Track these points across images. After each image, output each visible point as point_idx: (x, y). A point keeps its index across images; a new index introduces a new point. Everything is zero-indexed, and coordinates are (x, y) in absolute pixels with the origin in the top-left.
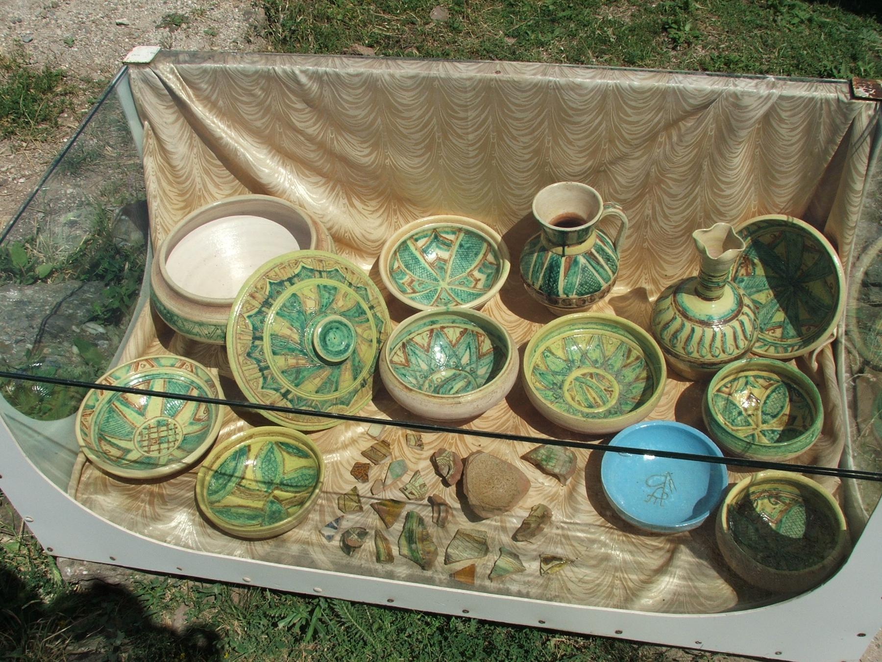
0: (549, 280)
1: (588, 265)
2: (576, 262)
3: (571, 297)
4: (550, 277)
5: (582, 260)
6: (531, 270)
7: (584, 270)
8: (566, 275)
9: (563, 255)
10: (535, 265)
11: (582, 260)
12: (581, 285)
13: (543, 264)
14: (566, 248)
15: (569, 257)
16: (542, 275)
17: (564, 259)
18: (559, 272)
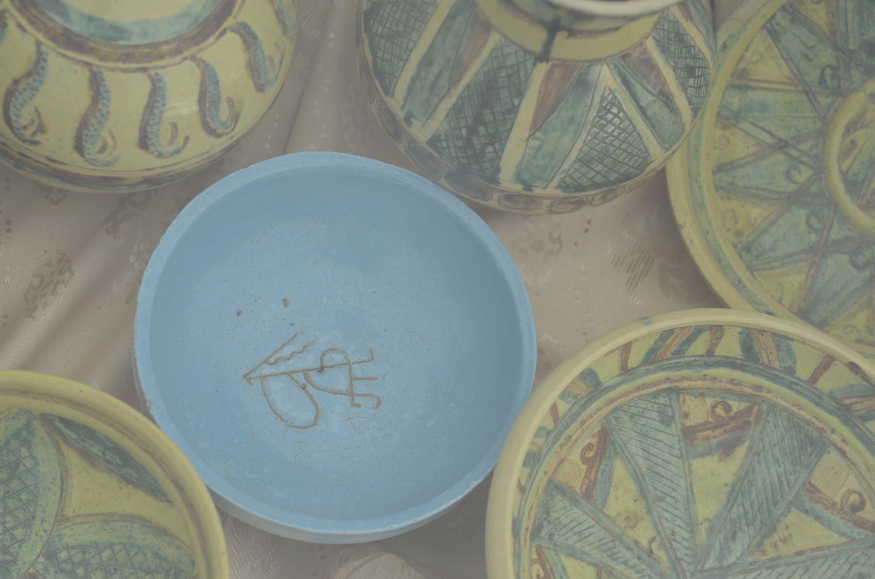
0: (472, 130)
1: (622, 96)
2: (583, 84)
3: (537, 191)
4: (479, 120)
5: (606, 78)
6: (410, 70)
7: (608, 105)
8: (537, 126)
9: (544, 56)
10: (426, 62)
11: (606, 78)
12: (584, 161)
13: (459, 69)
14: (561, 38)
15: (566, 65)
16: (448, 104)
17: (542, 69)
18: (514, 110)
